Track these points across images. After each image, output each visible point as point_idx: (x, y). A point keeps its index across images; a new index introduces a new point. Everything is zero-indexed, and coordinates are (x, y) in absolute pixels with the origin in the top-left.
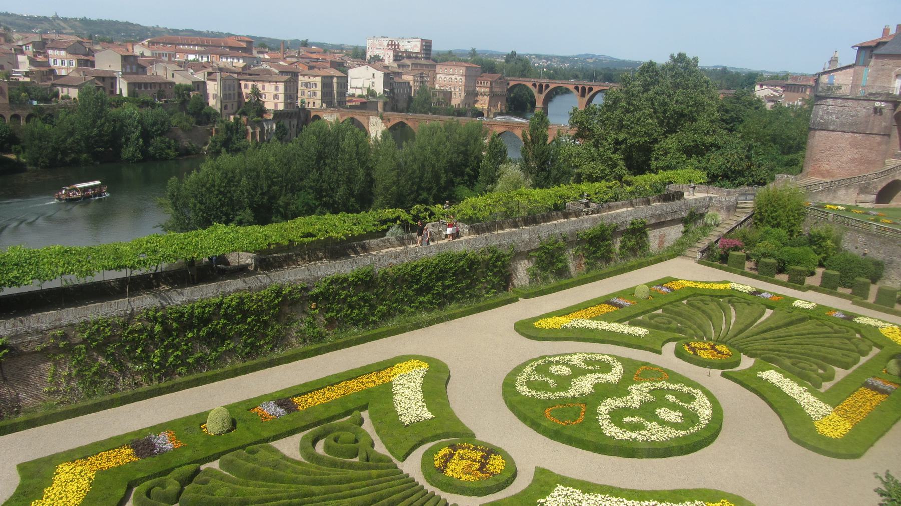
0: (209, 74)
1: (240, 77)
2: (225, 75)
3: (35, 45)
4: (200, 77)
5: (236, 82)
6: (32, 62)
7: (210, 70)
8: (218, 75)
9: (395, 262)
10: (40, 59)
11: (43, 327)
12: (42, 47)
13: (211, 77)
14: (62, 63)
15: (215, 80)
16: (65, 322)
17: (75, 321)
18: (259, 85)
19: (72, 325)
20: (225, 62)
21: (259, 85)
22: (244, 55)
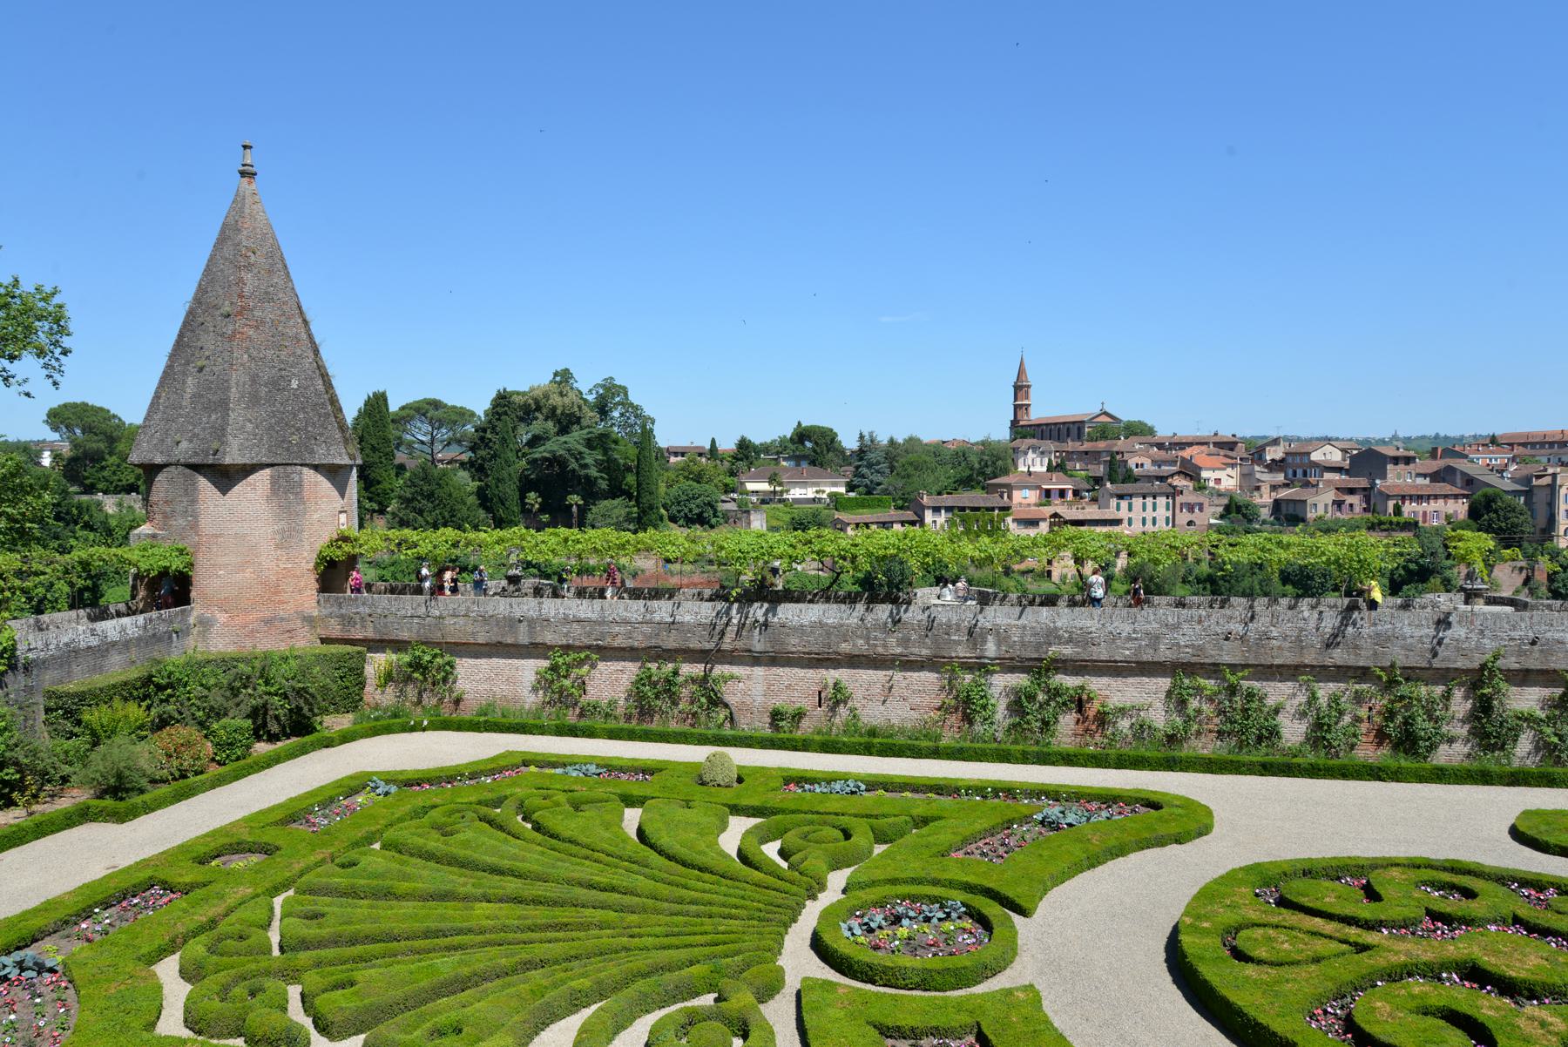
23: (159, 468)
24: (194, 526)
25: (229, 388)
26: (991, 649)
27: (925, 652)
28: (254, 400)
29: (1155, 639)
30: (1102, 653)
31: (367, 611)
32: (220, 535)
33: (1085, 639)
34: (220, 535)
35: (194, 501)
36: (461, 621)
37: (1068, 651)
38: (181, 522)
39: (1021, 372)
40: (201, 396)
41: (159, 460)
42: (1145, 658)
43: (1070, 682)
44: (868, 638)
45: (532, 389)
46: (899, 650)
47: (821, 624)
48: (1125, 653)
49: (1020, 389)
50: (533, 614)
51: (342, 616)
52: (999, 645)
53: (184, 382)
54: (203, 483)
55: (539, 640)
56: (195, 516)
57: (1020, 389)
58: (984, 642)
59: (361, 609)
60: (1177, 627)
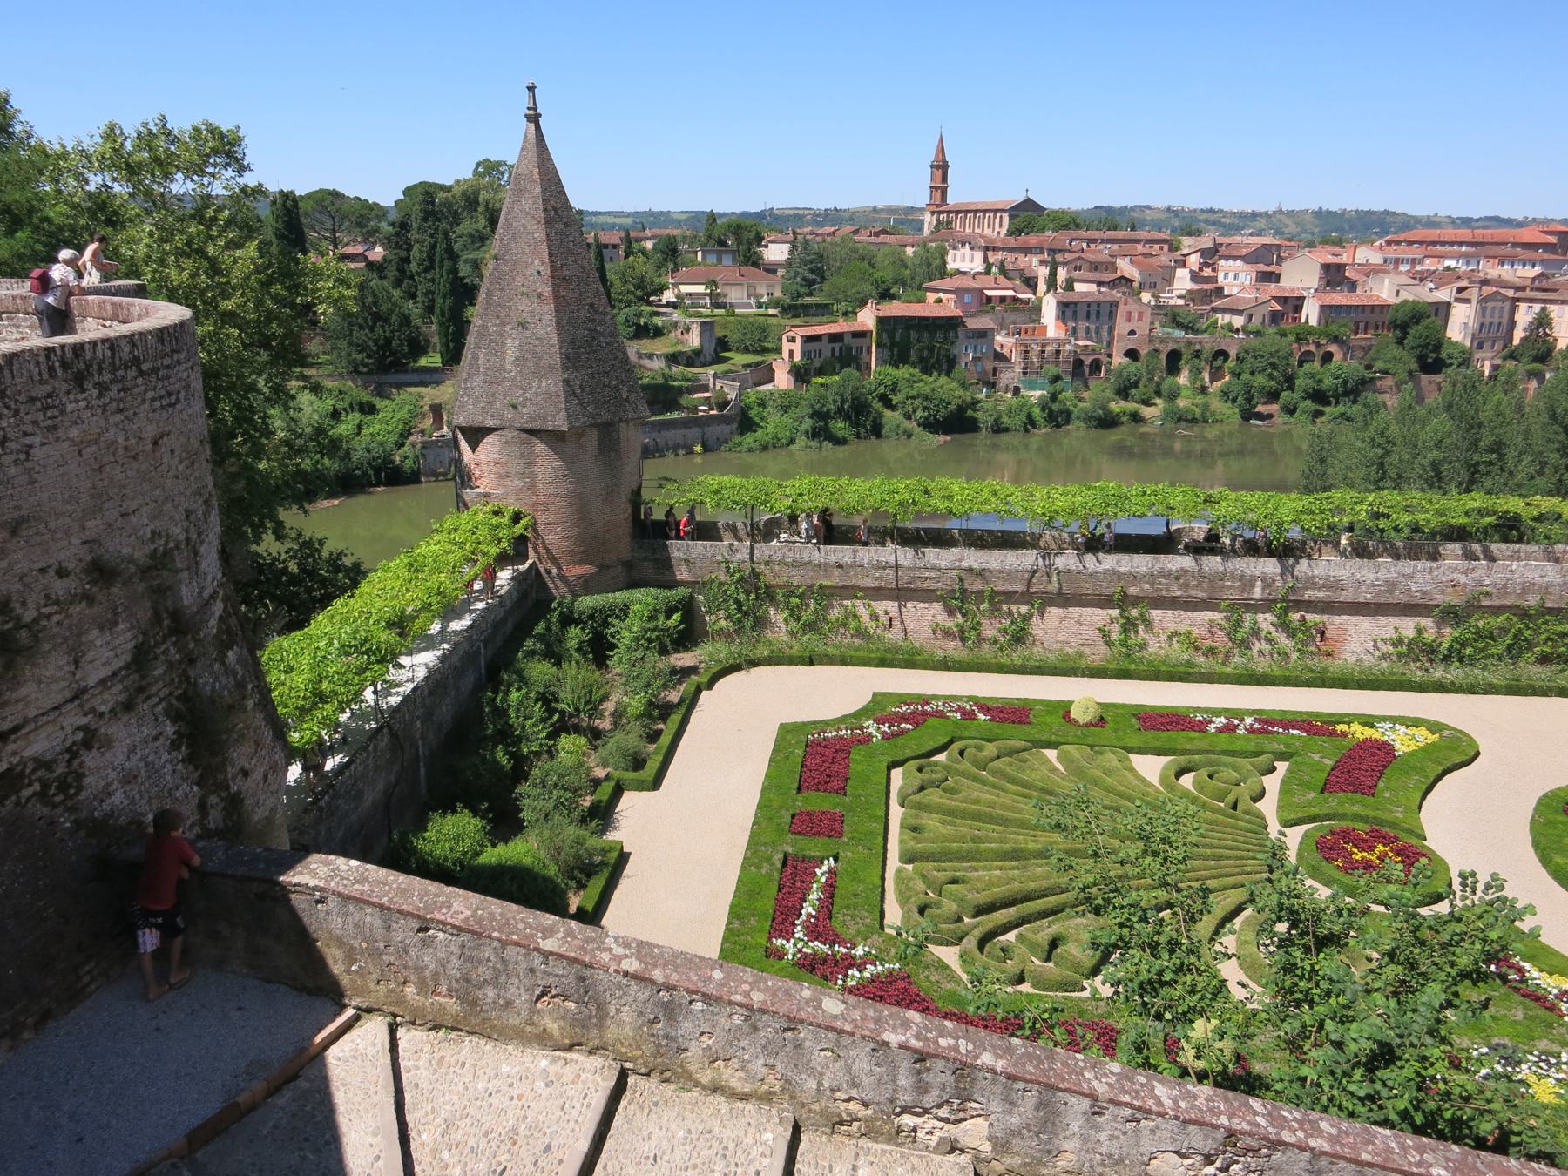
0: (1460, 290)
1: (1519, 294)
2: (1487, 290)
3: (1204, 253)
4: (1444, 295)
5: (1507, 305)
6: (1195, 277)
7: (1464, 284)
8: (1474, 294)
9: (1463, 579)
10: (1207, 272)
11: (943, 564)
12: (1211, 255)
13: (1464, 295)
14: (1236, 279)
15: (1468, 301)
16: (965, 564)
17: (976, 566)
18: (1554, 310)
19: (971, 569)
20: (1505, 272)
21: (1552, 307)
22: (1546, 256)
23: (489, 431)
26: (1257, 593)
27: (1201, 595)
29: (1392, 585)
30: (1345, 596)
33: (1334, 585)
37: (1321, 594)
39: (941, 150)
41: (490, 423)
42: (1382, 600)
43: (1311, 618)
44: (1152, 584)
45: (458, 182)
46: (1179, 593)
47: (1114, 572)
48: (1366, 596)
49: (941, 167)
50: (848, 560)
52: (1263, 589)
53: (504, 345)
54: (540, 446)
55: (848, 583)
57: (941, 167)
58: (1252, 587)
60: (1410, 577)
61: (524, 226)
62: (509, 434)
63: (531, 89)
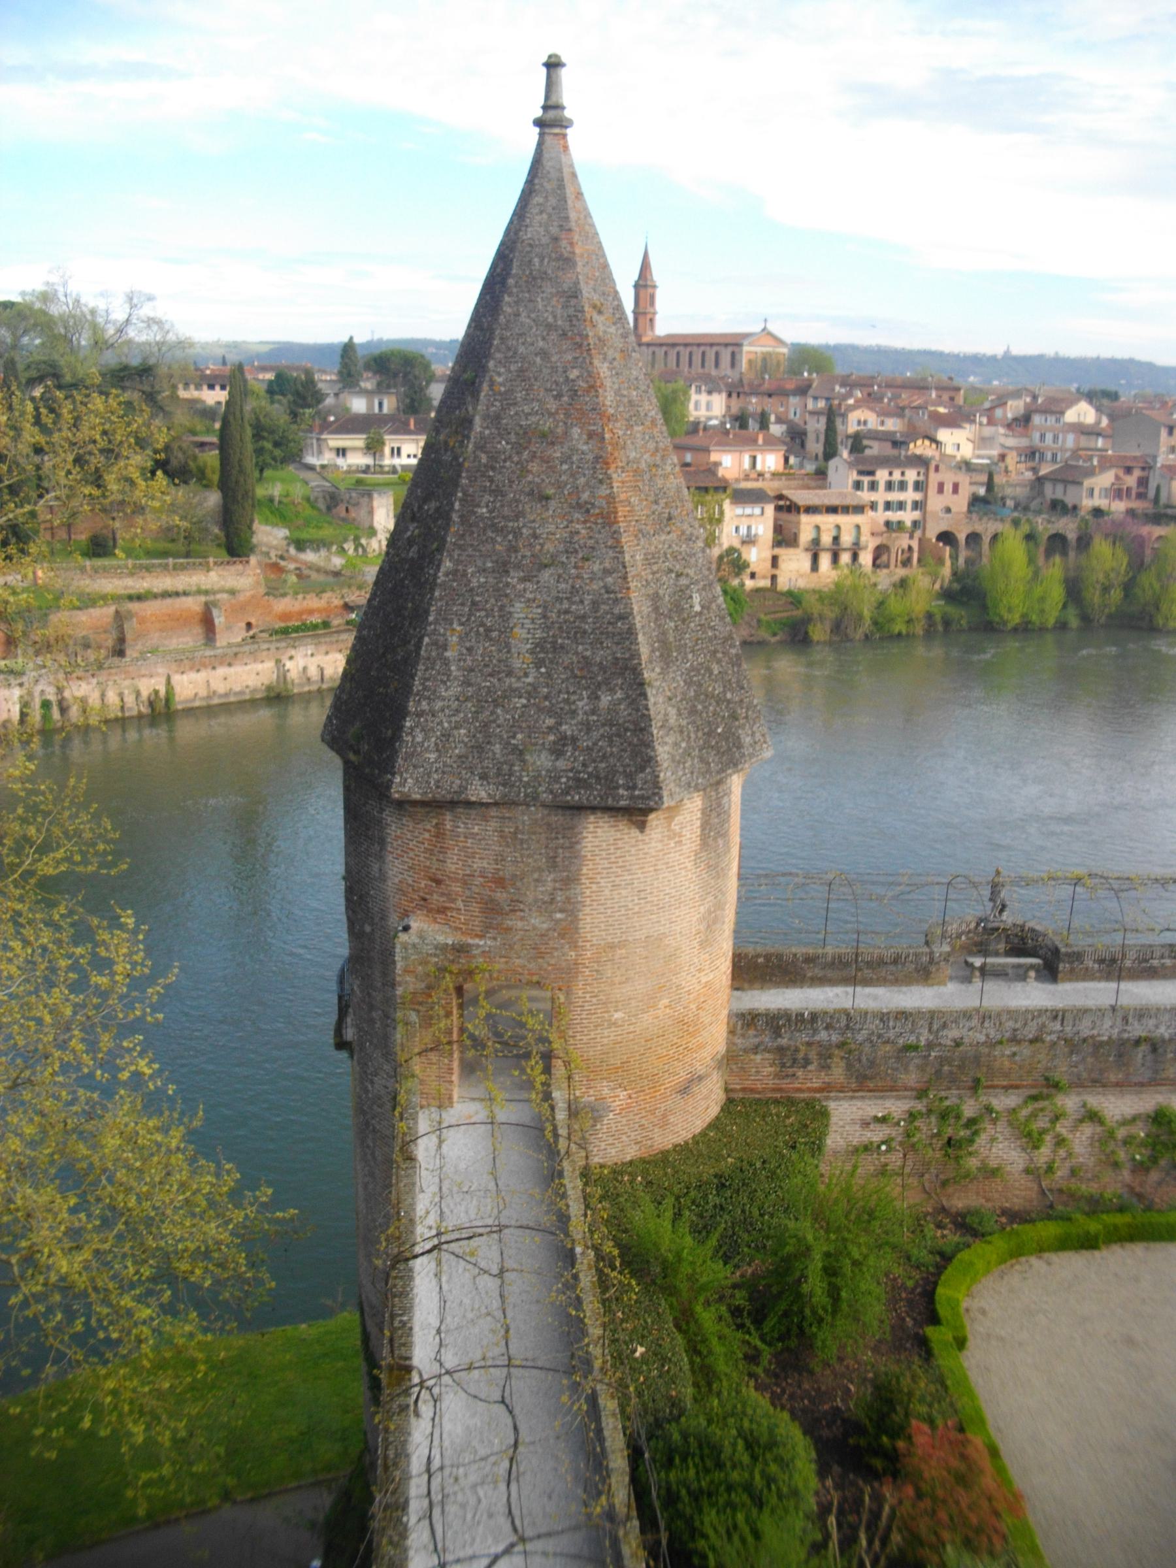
24: (569, 931)
25: (631, 632)
28: (666, 652)
31: (835, 1038)
32: (622, 944)
34: (622, 944)
35: (570, 881)
36: (1026, 1051)
38: (538, 922)
39: (645, 267)
40: (557, 648)
41: (479, 792)
51: (781, 1050)
53: (505, 616)
56: (572, 909)
59: (823, 1035)
61: (544, 354)
62: (525, 818)
63: (553, 65)
